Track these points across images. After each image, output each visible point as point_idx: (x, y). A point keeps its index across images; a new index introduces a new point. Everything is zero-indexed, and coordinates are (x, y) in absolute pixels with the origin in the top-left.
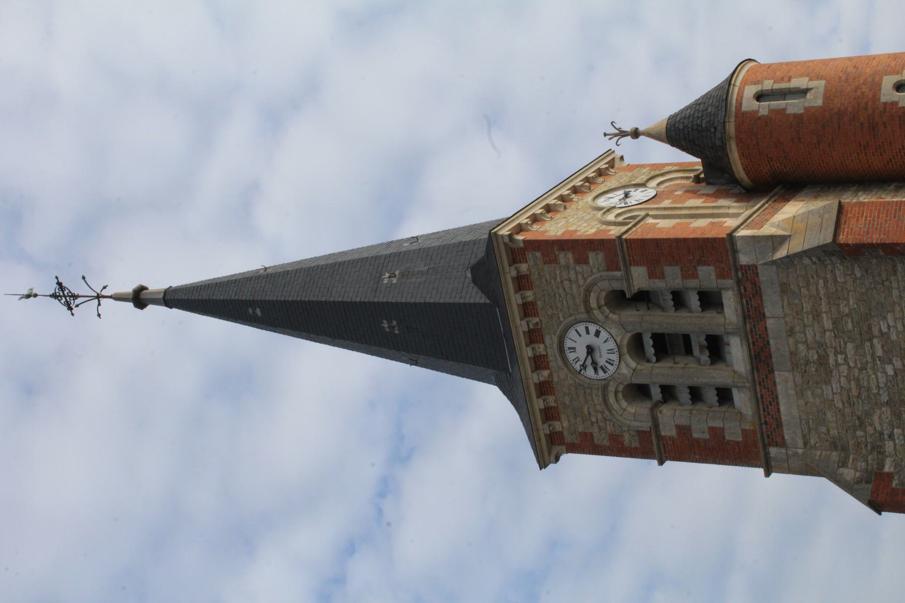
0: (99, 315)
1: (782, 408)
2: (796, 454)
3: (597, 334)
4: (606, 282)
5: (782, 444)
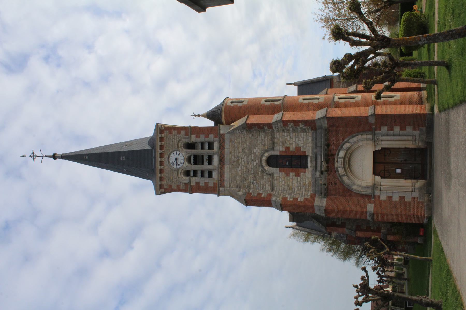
0: (42, 162)
1: (225, 175)
2: (227, 190)
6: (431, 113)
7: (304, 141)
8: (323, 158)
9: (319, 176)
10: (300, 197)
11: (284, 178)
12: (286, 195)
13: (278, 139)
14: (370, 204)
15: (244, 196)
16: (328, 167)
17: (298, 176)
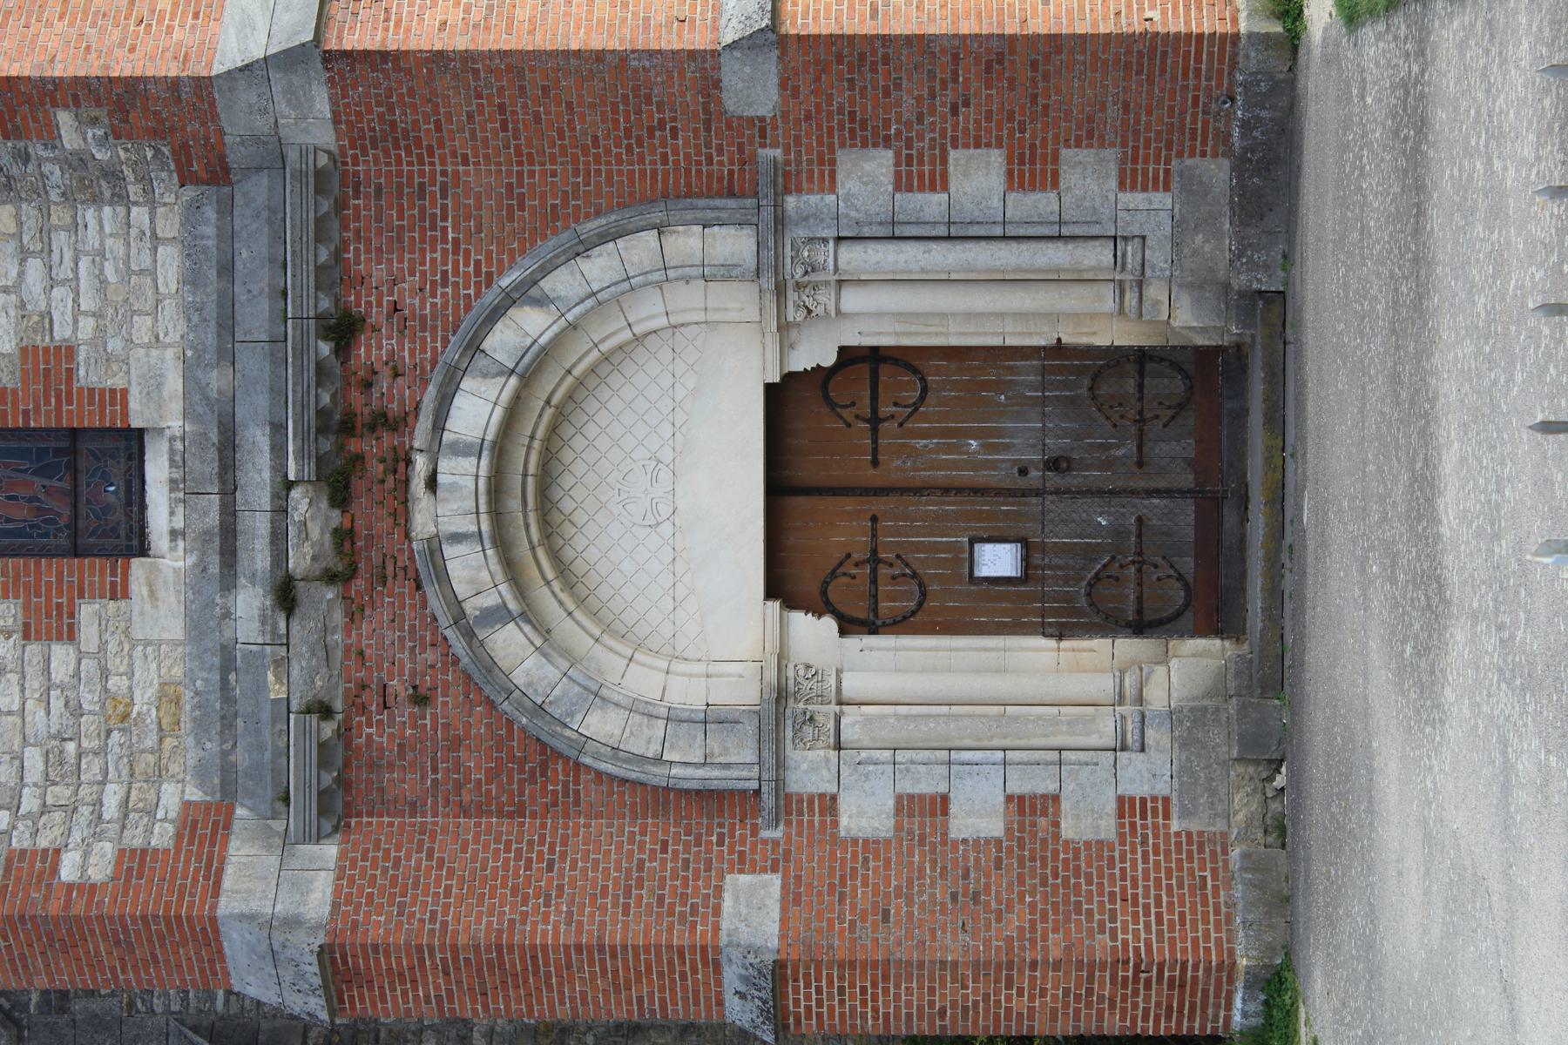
6: (1277, 28)
8: (300, 455)
9: (256, 625)
10: (76, 836)
14: (744, 879)
16: (343, 537)
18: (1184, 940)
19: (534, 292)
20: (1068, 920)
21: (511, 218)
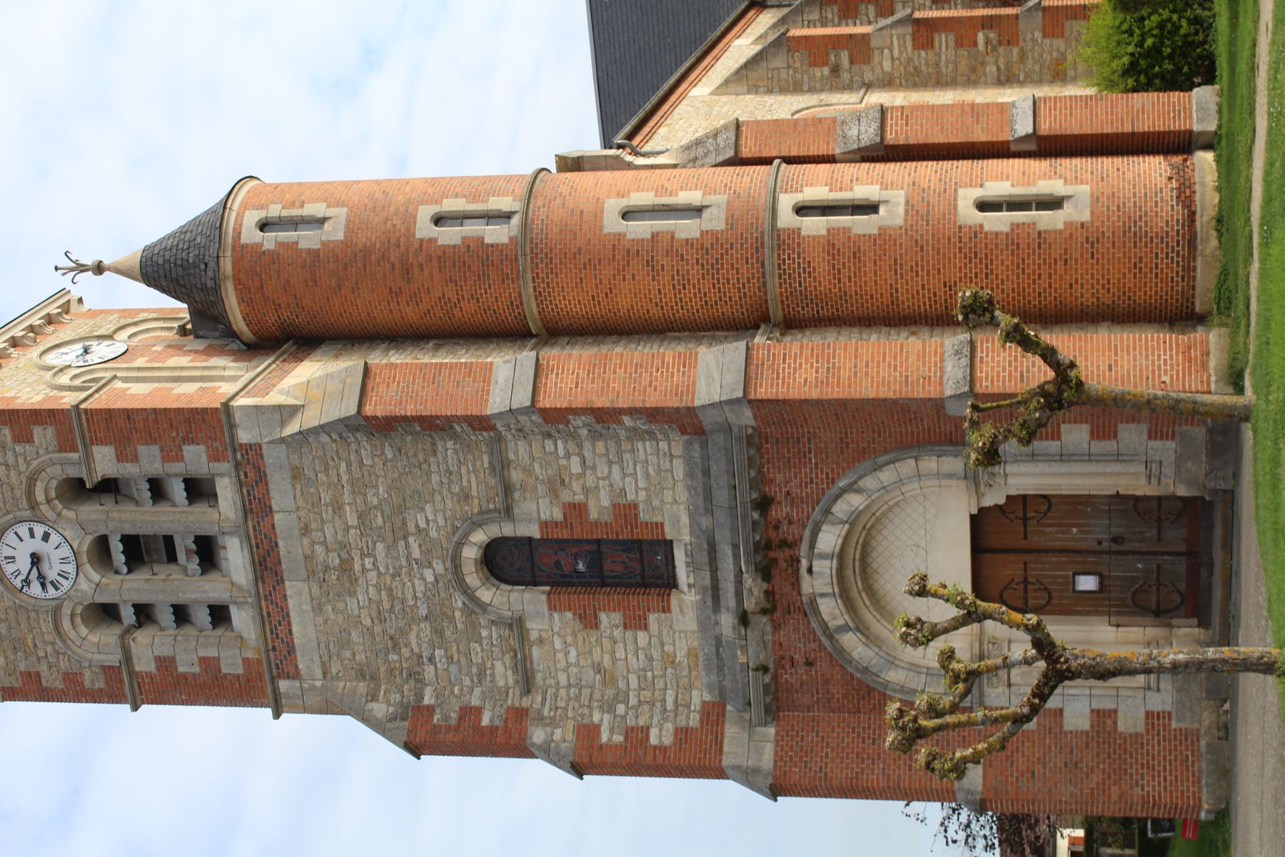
1: (295, 629)
2: (313, 688)
3: (46, 537)
4: (58, 468)
5: (296, 675)
7: (648, 476)
8: (747, 563)
9: (731, 630)
10: (655, 720)
11: (574, 635)
12: (591, 716)
13: (528, 471)
15: (397, 723)
16: (769, 594)
17: (636, 628)
18: (1177, 791)
19: (855, 487)
20: (1120, 779)
21: (842, 452)
